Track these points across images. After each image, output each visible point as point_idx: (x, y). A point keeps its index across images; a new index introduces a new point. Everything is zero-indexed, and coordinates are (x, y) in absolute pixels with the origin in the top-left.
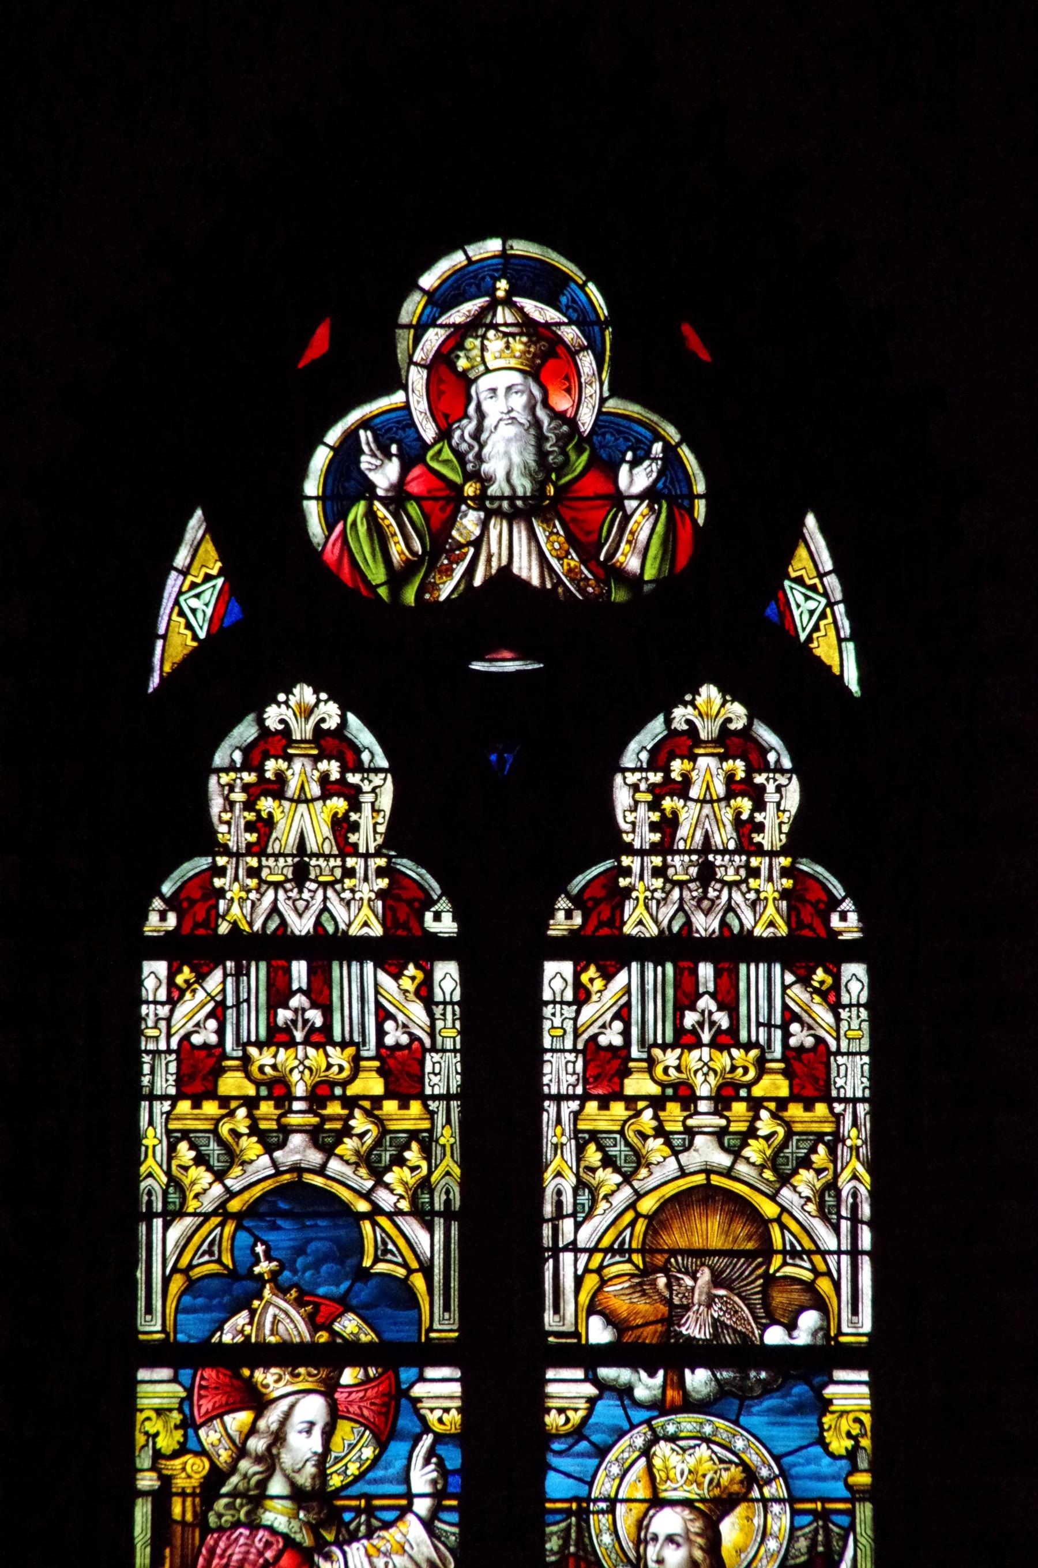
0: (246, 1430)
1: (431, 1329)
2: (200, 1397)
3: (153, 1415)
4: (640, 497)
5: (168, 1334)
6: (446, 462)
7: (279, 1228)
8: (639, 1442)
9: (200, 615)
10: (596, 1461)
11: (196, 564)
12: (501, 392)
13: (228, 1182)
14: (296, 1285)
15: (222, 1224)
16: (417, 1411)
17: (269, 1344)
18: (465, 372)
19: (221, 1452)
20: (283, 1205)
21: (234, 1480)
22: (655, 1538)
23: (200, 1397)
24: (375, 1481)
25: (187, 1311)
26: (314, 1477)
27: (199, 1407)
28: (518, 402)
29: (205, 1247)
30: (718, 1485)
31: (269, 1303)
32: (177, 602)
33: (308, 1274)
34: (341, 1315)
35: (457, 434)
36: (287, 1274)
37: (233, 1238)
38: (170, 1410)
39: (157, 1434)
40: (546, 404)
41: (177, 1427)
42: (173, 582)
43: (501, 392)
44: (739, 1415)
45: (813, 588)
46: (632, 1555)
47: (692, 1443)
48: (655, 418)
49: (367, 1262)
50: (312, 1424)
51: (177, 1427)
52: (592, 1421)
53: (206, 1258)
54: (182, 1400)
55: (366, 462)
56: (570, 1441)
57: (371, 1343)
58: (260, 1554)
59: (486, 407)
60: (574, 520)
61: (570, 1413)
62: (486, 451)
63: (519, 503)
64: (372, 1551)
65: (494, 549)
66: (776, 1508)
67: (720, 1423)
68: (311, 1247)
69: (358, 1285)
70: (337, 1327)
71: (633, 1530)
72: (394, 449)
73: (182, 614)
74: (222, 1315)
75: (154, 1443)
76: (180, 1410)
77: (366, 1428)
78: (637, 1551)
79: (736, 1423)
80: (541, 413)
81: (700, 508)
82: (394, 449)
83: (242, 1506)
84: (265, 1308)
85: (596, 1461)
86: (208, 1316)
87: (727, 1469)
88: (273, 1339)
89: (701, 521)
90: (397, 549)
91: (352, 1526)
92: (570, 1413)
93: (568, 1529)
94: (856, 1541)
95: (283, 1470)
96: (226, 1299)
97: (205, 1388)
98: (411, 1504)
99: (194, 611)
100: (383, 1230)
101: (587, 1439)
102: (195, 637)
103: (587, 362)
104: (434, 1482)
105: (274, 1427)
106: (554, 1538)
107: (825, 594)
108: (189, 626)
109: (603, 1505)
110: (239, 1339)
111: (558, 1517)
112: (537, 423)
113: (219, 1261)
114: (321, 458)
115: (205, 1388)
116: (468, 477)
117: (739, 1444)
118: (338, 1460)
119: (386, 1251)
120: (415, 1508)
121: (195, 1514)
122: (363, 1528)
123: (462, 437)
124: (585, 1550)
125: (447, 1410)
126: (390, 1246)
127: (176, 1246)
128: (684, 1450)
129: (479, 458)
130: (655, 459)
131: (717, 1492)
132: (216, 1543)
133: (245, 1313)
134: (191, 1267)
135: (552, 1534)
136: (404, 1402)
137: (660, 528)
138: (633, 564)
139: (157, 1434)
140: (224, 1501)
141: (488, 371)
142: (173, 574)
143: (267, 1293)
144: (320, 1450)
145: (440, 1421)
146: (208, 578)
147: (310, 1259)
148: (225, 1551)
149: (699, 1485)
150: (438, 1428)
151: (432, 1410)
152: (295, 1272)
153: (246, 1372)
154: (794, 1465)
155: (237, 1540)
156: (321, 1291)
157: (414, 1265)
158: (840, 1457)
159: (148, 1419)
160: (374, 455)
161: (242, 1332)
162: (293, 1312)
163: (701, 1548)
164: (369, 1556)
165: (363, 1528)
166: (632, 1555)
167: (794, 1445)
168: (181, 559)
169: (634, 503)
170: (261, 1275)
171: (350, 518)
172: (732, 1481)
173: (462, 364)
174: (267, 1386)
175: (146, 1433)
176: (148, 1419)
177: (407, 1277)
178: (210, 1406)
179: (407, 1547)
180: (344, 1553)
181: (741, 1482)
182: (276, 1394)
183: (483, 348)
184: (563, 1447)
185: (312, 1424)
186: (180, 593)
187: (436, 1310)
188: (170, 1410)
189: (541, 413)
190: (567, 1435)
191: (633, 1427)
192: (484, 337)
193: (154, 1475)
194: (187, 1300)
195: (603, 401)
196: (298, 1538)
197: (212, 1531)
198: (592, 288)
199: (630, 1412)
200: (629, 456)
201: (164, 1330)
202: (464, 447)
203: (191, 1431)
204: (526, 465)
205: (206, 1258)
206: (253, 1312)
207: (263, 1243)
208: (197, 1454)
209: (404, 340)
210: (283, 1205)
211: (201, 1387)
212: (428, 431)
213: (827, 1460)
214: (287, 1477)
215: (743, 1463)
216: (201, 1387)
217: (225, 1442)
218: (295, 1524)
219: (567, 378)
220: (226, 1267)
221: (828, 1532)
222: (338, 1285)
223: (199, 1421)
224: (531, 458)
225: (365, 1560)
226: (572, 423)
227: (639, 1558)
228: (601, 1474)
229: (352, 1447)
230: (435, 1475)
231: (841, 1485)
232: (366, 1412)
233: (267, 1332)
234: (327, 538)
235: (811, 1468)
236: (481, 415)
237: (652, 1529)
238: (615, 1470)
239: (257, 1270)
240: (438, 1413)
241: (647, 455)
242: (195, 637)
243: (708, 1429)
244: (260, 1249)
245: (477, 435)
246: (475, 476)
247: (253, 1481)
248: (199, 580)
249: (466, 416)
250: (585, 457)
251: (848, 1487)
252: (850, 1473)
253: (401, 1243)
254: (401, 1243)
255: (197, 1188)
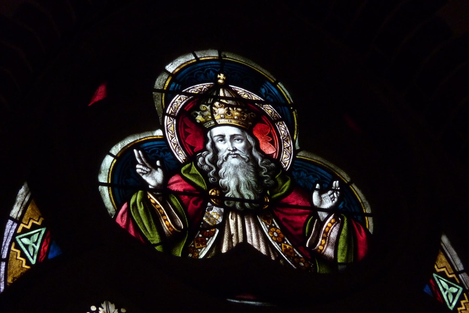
4: (329, 211)
6: (194, 175)
9: (31, 250)
11: (26, 217)
12: (227, 138)
18: (201, 123)
28: (239, 145)
32: (13, 240)
35: (201, 159)
40: (258, 148)
42: (10, 227)
43: (227, 138)
45: (452, 280)
48: (332, 166)
55: (139, 168)
59: (219, 145)
60: (285, 220)
62: (222, 171)
63: (247, 205)
65: (233, 231)
72: (158, 163)
73: (17, 247)
80: (255, 154)
81: (369, 222)
82: (158, 163)
89: (371, 230)
90: (166, 223)
99: (27, 246)
102: (28, 263)
103: (283, 129)
107: (461, 284)
108: (23, 255)
112: (252, 159)
114: (108, 161)
116: (211, 186)
123: (204, 161)
129: (217, 176)
130: (335, 191)
137: (344, 232)
138: (329, 251)
141: (217, 125)
142: (10, 222)
146: (34, 227)
160: (144, 165)
168: (15, 211)
169: (324, 215)
171: (132, 201)
173: (199, 118)
183: (213, 112)
186: (15, 234)
189: (255, 154)
192: (212, 105)
195: (296, 152)
198: (280, 85)
200: (318, 186)
202: (206, 167)
204: (249, 183)
209: (159, 101)
212: (181, 157)
219: (270, 135)
224: (252, 179)
226: (278, 162)
234: (117, 212)
236: (216, 151)
241: (330, 187)
242: (28, 263)
245: (215, 159)
246: (216, 185)
248: (29, 227)
249: (205, 149)
250: (288, 183)
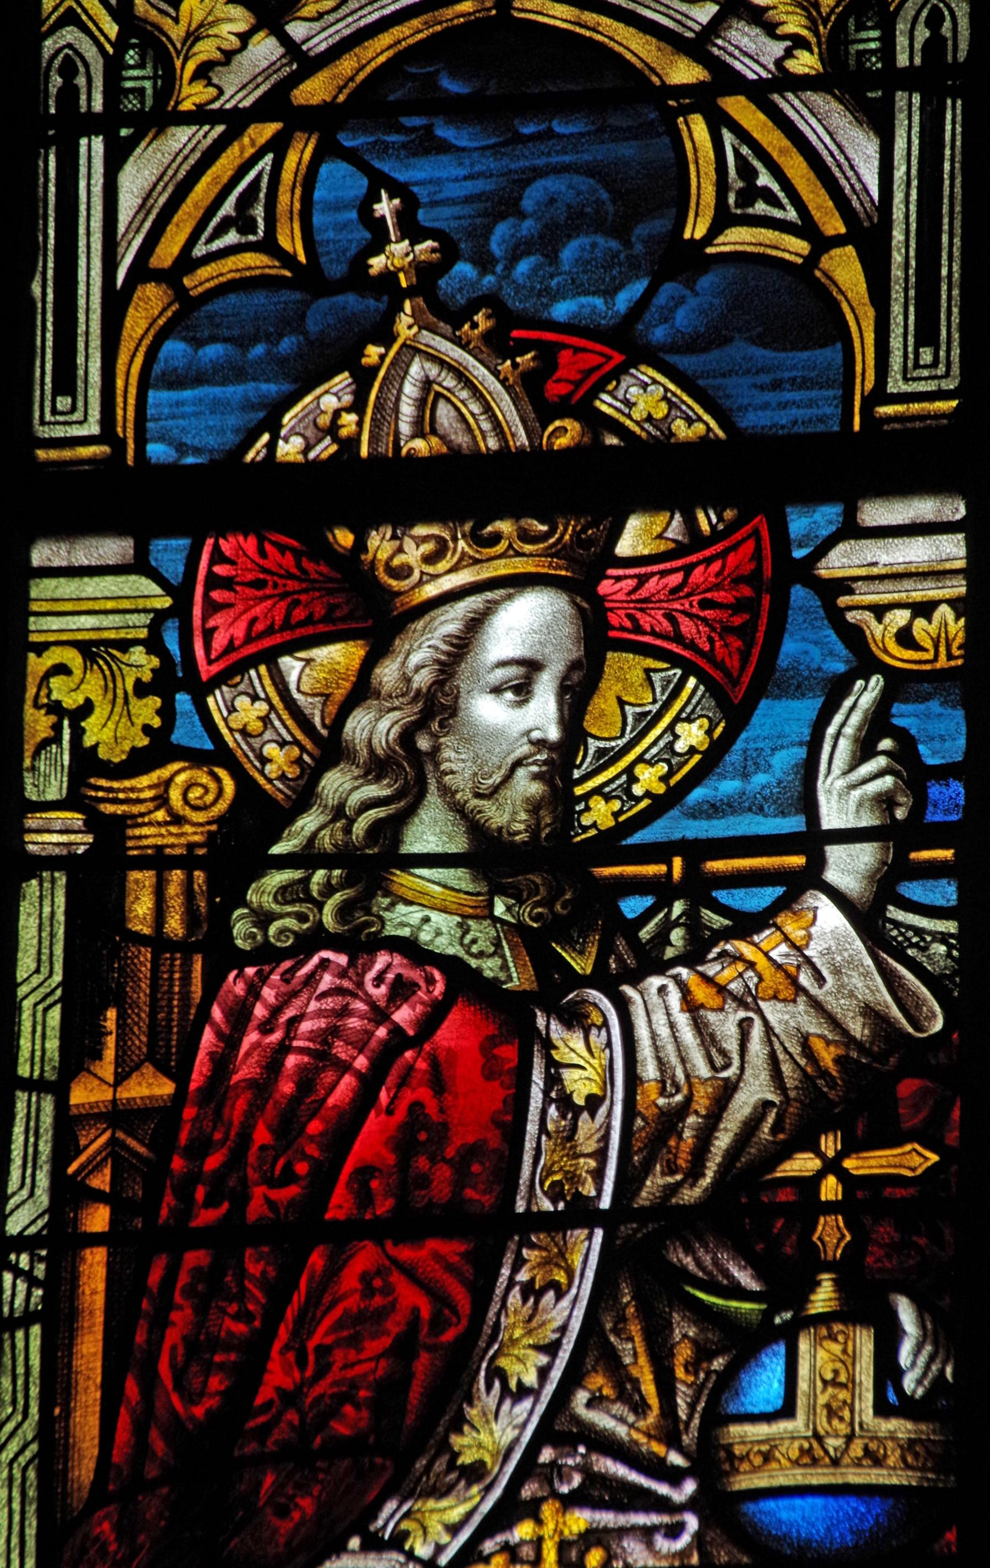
0: (339, 694)
1: (880, 395)
2: (211, 608)
3: (73, 658)
5: (119, 445)
7: (444, 147)
13: (296, 30)
14: (491, 301)
15: (279, 146)
16: (836, 617)
17: (412, 458)
19: (271, 750)
20: (451, 85)
21: (308, 823)
23: (211, 608)
24: (714, 810)
25: (175, 381)
26: (534, 807)
27: (208, 635)
29: (228, 207)
31: (411, 350)
33: (523, 267)
34: (618, 373)
36: (463, 269)
37: (309, 180)
38: (125, 645)
39: (87, 708)
41: (142, 690)
49: (696, 229)
50: (532, 666)
51: (142, 690)
53: (232, 237)
54: (160, 617)
57: (705, 441)
58: (379, 1014)
64: (701, 993)
68: (531, 198)
69: (668, 289)
70: (605, 404)
74: (271, 389)
75: (78, 733)
76: (153, 644)
77: (689, 669)
83: (329, 889)
84: (400, 368)
86: (234, 392)
88: (420, 445)
91: (645, 933)
95: (446, 792)
96: (287, 344)
97: (227, 583)
98: (818, 862)
100: (743, 135)
104: (885, 801)
105: (422, 679)
110: (325, 449)
113: (269, 245)
115: (227, 583)
118: (607, 758)
119: (751, 193)
120: (832, 876)
121: (191, 918)
122: (677, 936)
125: (924, 609)
126: (764, 179)
127: (144, 208)
132: (254, 992)
133: (342, 380)
134: (186, 263)
136: (799, 593)
139: (87, 708)
140: (277, 878)
143: (404, 325)
144: (553, 734)
145: (905, 637)
147: (528, 227)
148: (276, 1011)
150: (899, 657)
151: (879, 611)
152: (484, 262)
153: (344, 538)
155: (312, 980)
156: (562, 310)
157: (834, 225)
159: (62, 669)
161: (333, 429)
162: (479, 372)
164: (691, 1006)
165: (677, 936)
170: (389, 276)
174: (403, 572)
175: (55, 708)
176: (62, 669)
177: (812, 260)
178: (239, 631)
179: (805, 979)
180: (623, 1006)
182: (431, 590)
185: (532, 666)
187: (896, 343)
188: (125, 645)
193: (75, 818)
194: (174, 348)
196: (490, 968)
197: (241, 959)
201: (108, 433)
203: (183, 701)
205: (232, 237)
206: (364, 377)
207: (396, 189)
208: (195, 758)
210: (451, 85)
211: (213, 581)
214: (459, 809)
216: (213, 581)
217: (285, 726)
218: (481, 933)
220: (287, 259)
222: (610, 293)
223: (206, 671)
225: (682, 1020)
229: (648, 721)
230: (888, 781)
232: (687, 626)
233: (405, 428)
239: (377, 263)
240: (900, 617)
244: (385, 207)
247: (361, 826)
253: (796, 168)
254: (796, 168)
255: (206, 50)
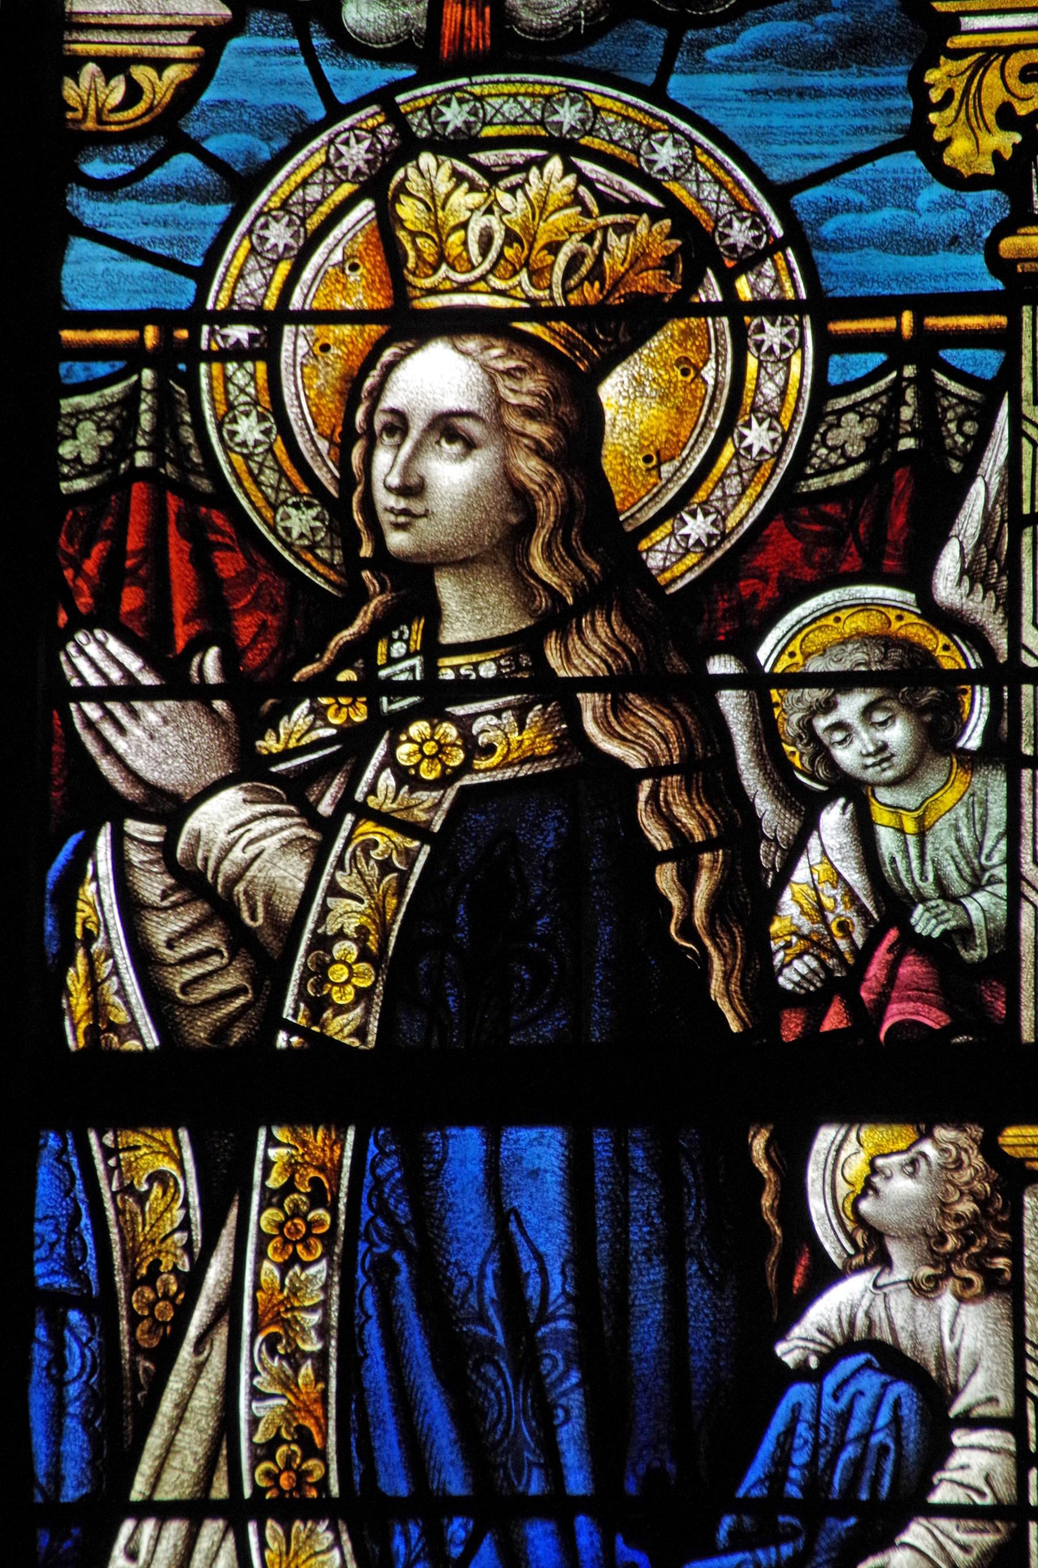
8: (356, 155)
10: (221, 211)
22: (399, 426)
30: (597, 272)
44: (665, 71)
46: (326, 475)
47: (518, 155)
52: (207, 97)
56: (143, 153)
61: (142, 74)
66: (774, 334)
67: (603, 94)
71: (331, 404)
78: (344, 463)
79: (657, 94)
85: (221, 211)
87: (623, 229)
92: (142, 74)
93: (131, 399)
94: (1016, 418)
101: (195, 148)
106: (87, 428)
109: (240, 333)
111: (101, 369)
117: (666, 155)
124: (181, 459)
128: (493, 176)
131: (591, 293)
135: (79, 414)
149: (536, 275)
154: (832, 209)
158: (978, 182)
163: (538, 450)
166: (326, 475)
167: (836, 153)
172: (638, 261)
181: (668, 263)
184: (119, 169)
190: (130, 137)
191: (336, 111)
199: (329, 71)
213: (938, 191)
215: (673, 207)
221: (928, 393)
227: (346, 481)
228: (237, 250)
231: (978, 261)
235: (885, 217)
237: (391, 400)
238: (279, 234)
243: (568, 115)
251: (997, 265)
252: (1006, 228)
